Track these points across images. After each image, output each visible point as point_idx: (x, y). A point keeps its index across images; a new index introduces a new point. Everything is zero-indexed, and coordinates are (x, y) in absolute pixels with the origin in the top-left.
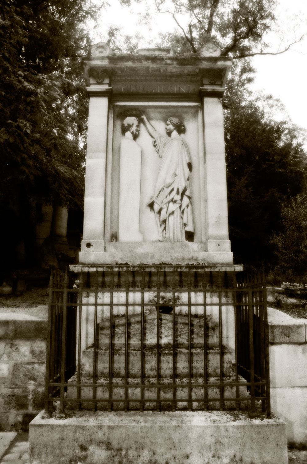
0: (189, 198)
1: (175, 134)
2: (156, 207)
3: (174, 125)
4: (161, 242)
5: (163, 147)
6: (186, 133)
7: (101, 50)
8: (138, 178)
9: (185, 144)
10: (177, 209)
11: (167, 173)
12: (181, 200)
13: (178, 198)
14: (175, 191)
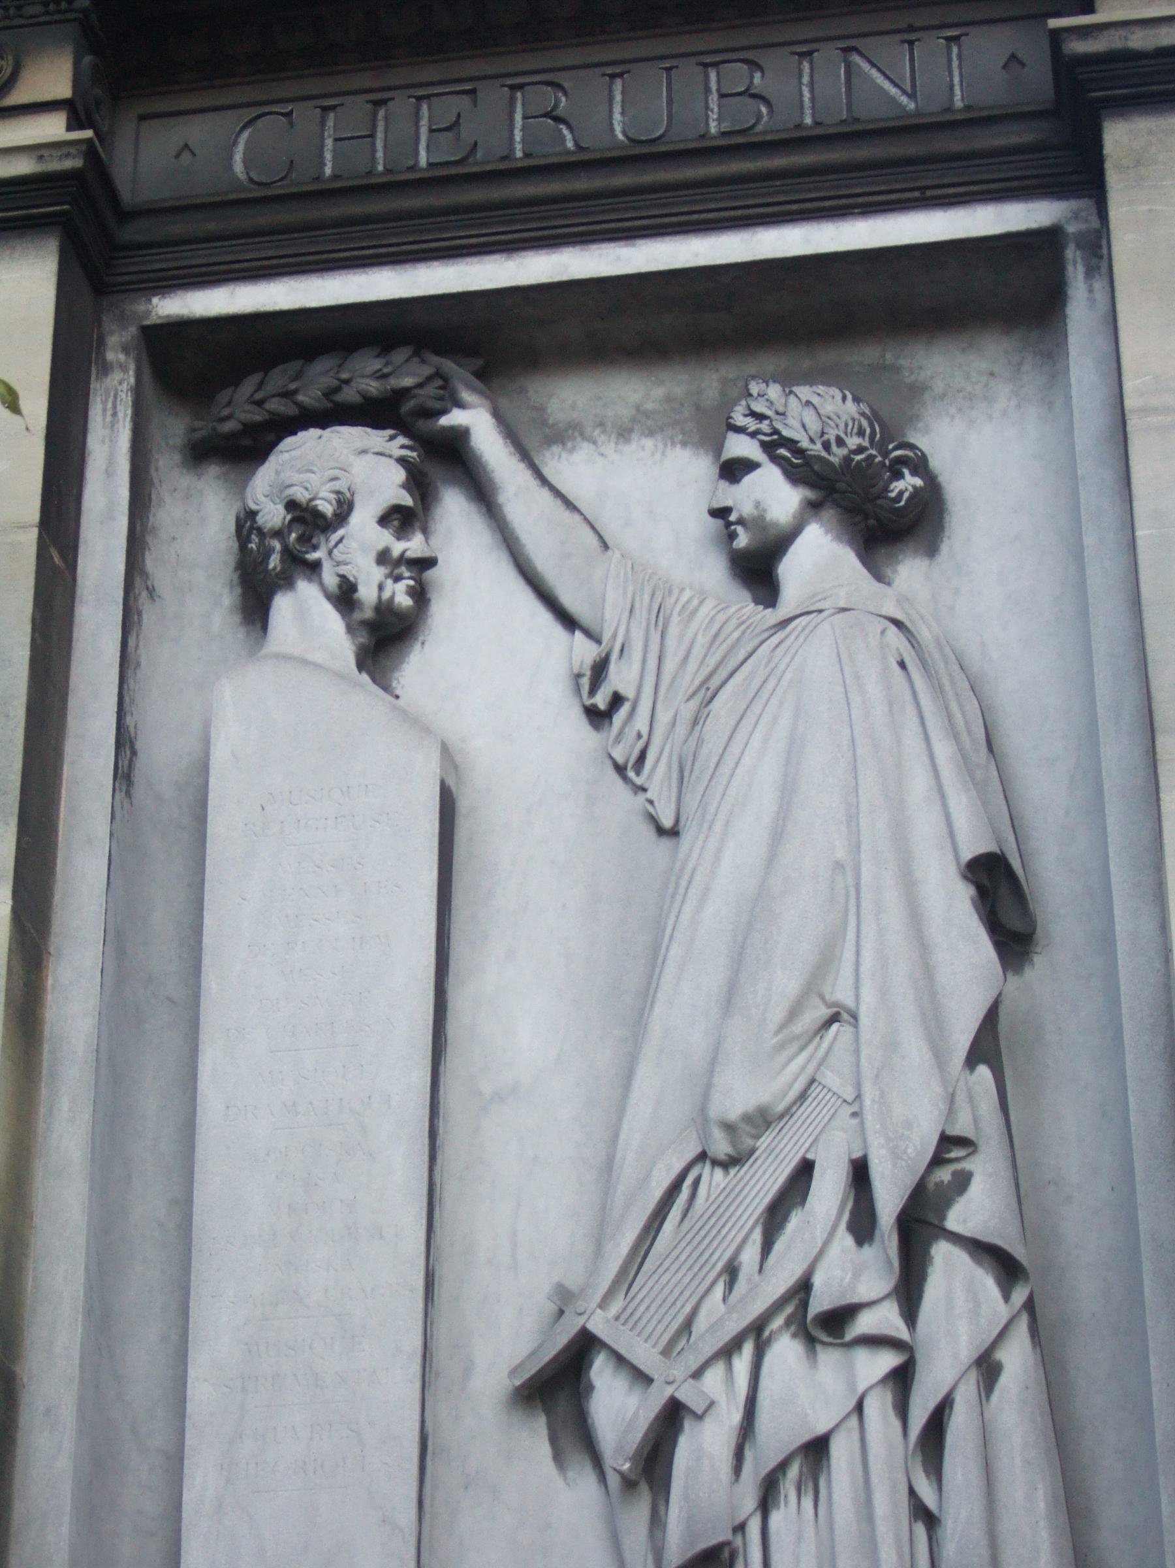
1: (818, 557)
2: (617, 1409)
3: (801, 467)
5: (687, 711)
6: (944, 548)
10: (859, 1407)
12: (909, 1291)
13: (855, 1273)
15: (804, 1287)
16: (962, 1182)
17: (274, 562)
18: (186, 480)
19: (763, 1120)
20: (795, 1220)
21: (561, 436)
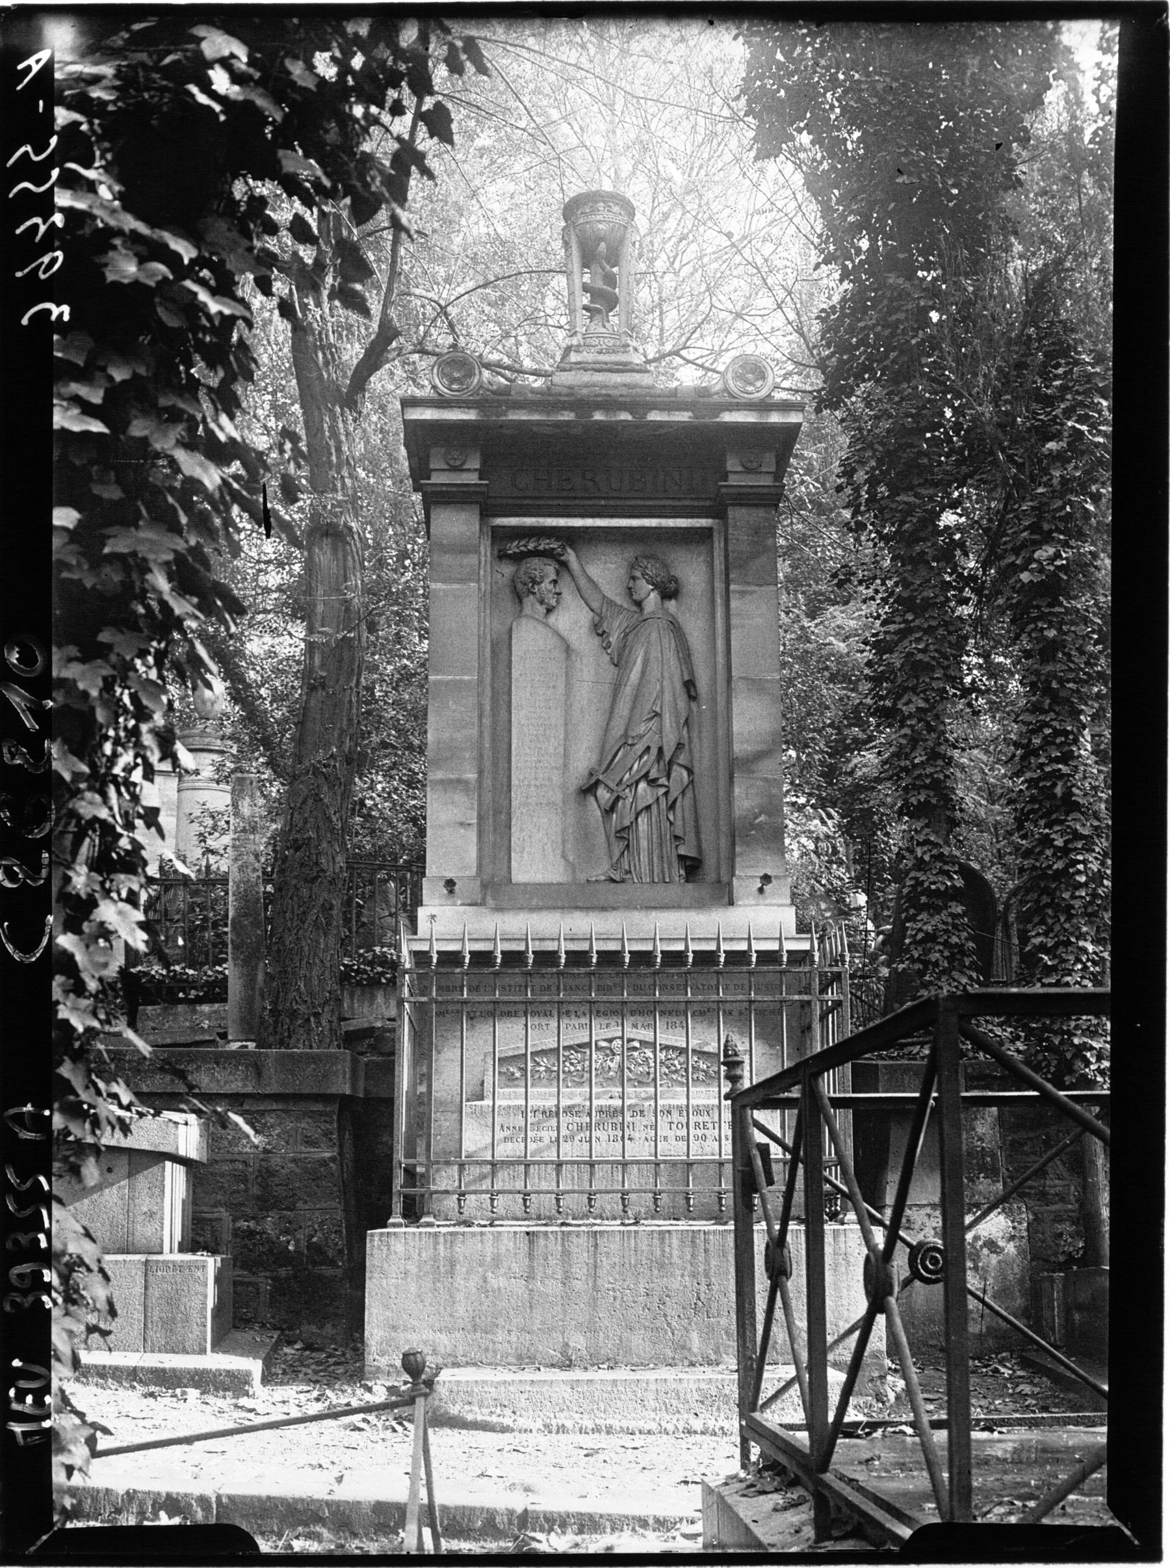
15: (648, 772)
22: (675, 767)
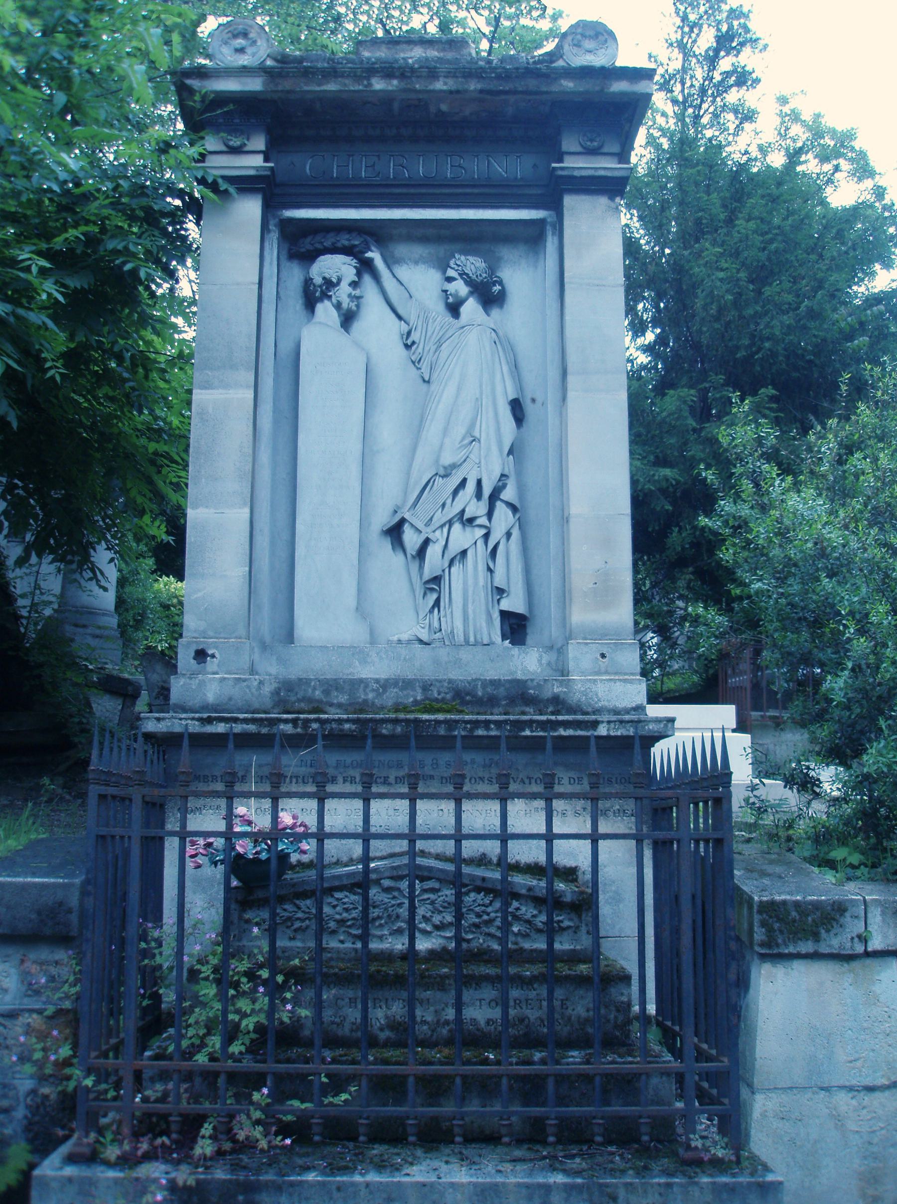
0: (514, 508)
1: (471, 308)
2: (411, 539)
3: (469, 282)
4: (426, 644)
5: (433, 348)
7: (240, 42)
8: (355, 446)
9: (502, 342)
11: (445, 432)
12: (490, 515)
13: (477, 509)
14: (471, 487)
15: (463, 512)
16: (504, 486)
17: (318, 294)
18: (288, 264)
19: (455, 466)
20: (461, 493)
21: (399, 261)
22: (499, 504)
